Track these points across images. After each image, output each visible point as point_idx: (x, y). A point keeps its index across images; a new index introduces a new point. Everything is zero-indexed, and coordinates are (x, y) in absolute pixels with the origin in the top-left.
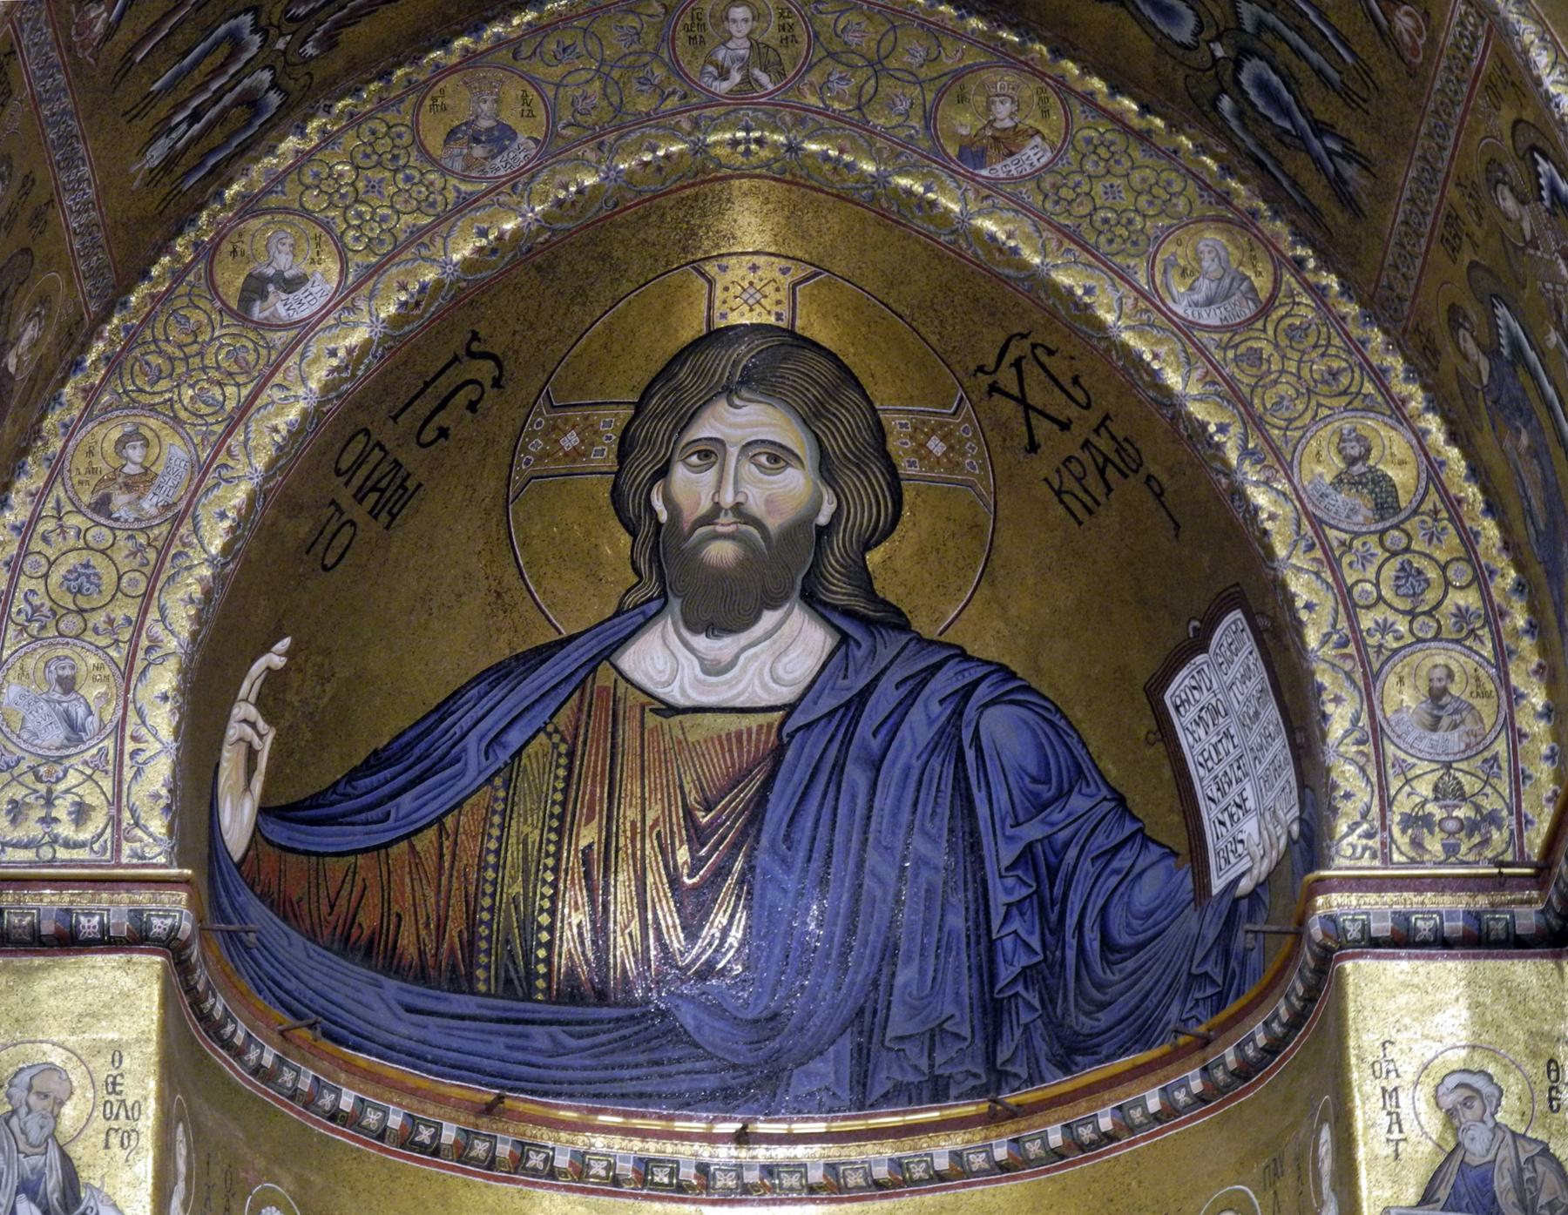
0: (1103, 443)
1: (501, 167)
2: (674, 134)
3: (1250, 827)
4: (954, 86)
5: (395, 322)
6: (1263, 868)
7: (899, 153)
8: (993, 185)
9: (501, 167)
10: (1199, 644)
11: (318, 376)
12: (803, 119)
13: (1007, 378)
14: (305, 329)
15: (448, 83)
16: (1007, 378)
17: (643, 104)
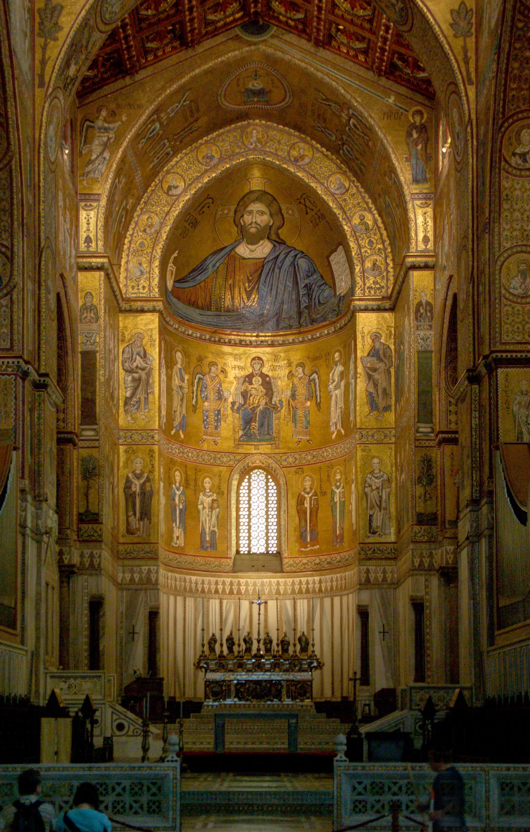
0: (319, 213)
1: (212, 163)
2: (243, 156)
3: (343, 284)
4: (293, 146)
5: (194, 194)
6: (345, 292)
7: (283, 159)
8: (299, 166)
9: (212, 163)
10: (335, 250)
11: (181, 205)
12: (265, 153)
13: (302, 201)
14: (179, 196)
15: (203, 147)
16: (302, 201)
17: (237, 151)
